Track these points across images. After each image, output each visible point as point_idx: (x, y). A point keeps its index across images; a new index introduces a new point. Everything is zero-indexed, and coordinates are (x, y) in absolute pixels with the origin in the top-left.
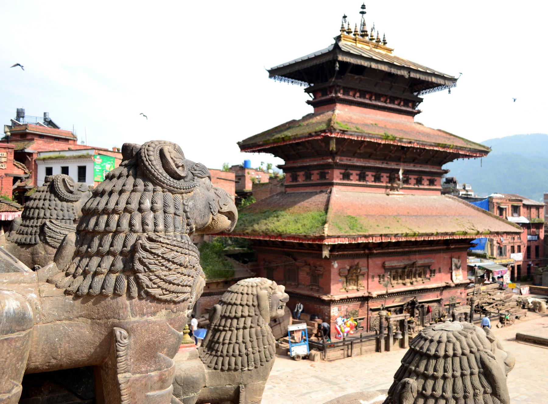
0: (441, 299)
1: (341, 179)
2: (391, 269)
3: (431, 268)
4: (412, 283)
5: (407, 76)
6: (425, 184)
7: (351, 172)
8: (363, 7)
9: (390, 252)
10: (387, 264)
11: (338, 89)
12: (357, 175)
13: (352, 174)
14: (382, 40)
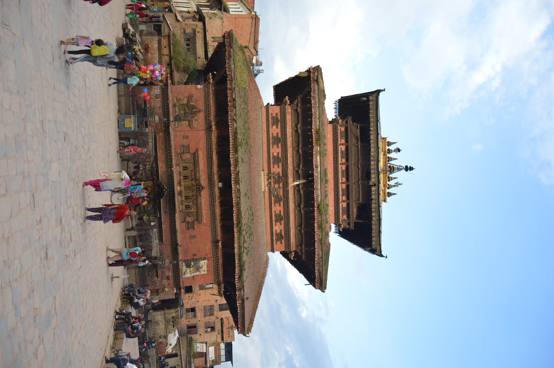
0: (162, 242)
1: (272, 114)
2: (196, 163)
3: (196, 223)
4: (180, 193)
5: (371, 183)
6: (277, 228)
7: (279, 126)
8: (411, 169)
9: (212, 157)
10: (200, 153)
11: (344, 122)
12: (277, 134)
13: (277, 128)
14: (391, 191)
